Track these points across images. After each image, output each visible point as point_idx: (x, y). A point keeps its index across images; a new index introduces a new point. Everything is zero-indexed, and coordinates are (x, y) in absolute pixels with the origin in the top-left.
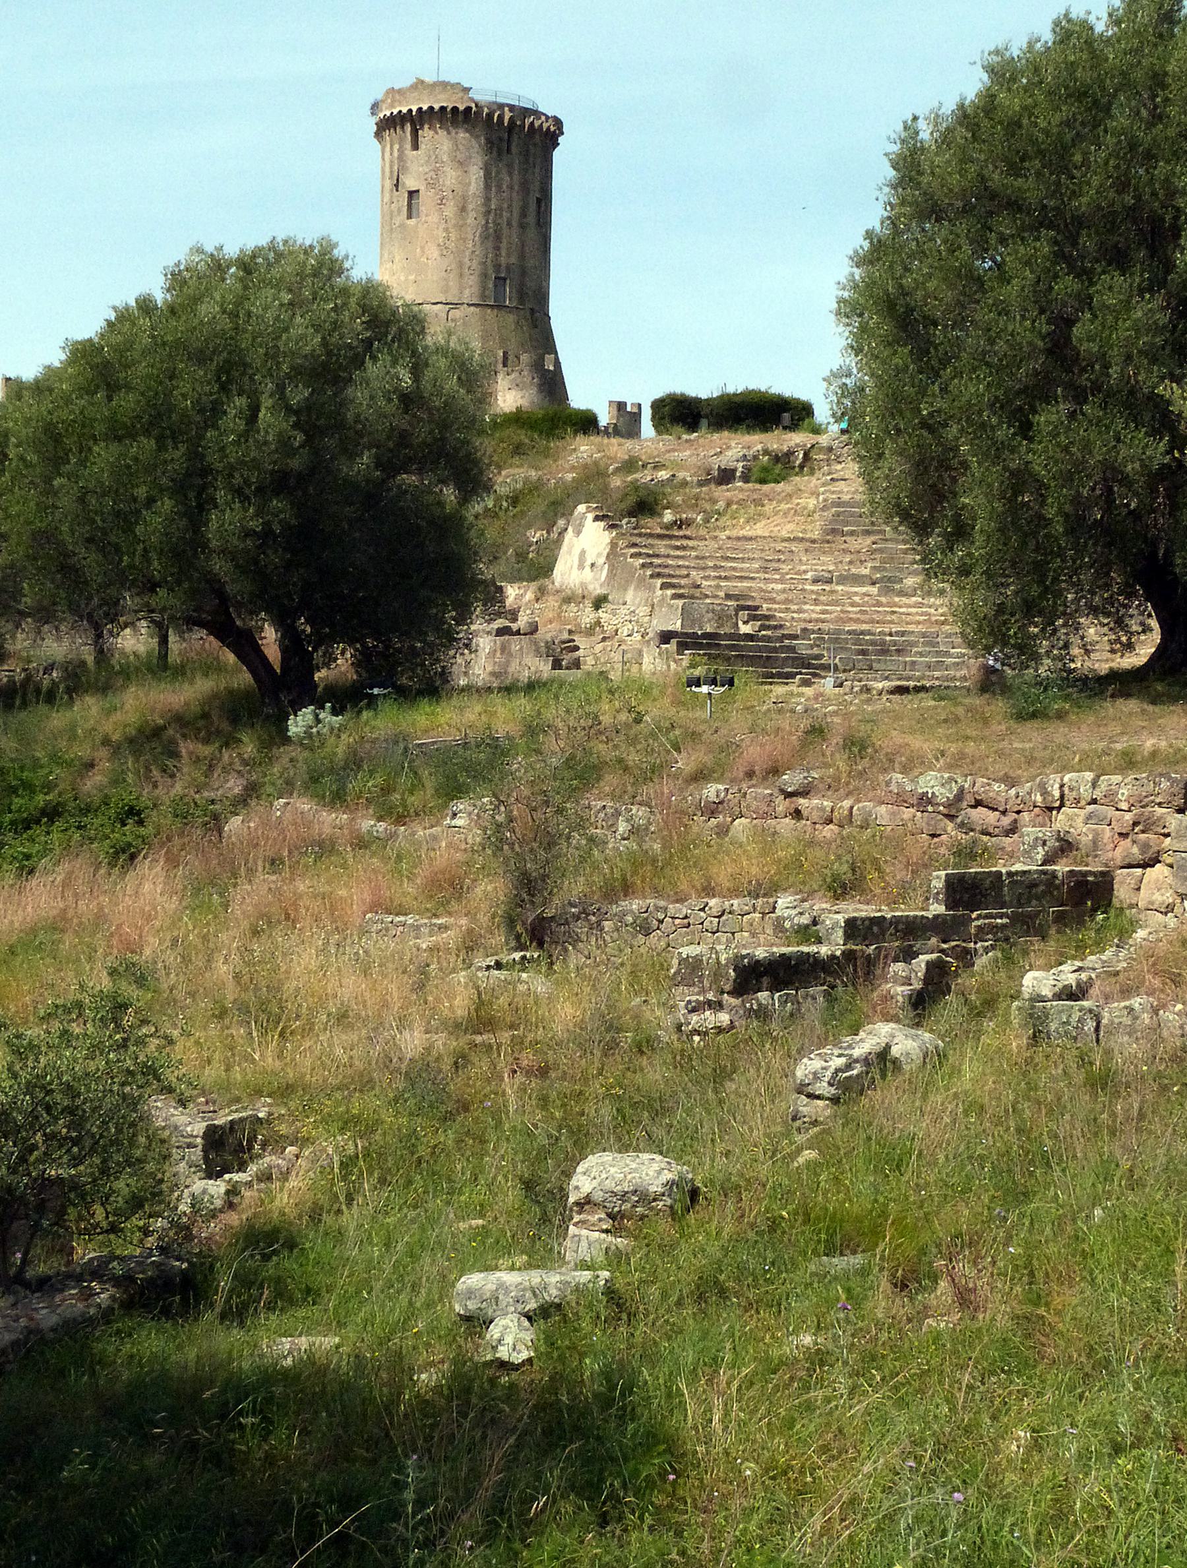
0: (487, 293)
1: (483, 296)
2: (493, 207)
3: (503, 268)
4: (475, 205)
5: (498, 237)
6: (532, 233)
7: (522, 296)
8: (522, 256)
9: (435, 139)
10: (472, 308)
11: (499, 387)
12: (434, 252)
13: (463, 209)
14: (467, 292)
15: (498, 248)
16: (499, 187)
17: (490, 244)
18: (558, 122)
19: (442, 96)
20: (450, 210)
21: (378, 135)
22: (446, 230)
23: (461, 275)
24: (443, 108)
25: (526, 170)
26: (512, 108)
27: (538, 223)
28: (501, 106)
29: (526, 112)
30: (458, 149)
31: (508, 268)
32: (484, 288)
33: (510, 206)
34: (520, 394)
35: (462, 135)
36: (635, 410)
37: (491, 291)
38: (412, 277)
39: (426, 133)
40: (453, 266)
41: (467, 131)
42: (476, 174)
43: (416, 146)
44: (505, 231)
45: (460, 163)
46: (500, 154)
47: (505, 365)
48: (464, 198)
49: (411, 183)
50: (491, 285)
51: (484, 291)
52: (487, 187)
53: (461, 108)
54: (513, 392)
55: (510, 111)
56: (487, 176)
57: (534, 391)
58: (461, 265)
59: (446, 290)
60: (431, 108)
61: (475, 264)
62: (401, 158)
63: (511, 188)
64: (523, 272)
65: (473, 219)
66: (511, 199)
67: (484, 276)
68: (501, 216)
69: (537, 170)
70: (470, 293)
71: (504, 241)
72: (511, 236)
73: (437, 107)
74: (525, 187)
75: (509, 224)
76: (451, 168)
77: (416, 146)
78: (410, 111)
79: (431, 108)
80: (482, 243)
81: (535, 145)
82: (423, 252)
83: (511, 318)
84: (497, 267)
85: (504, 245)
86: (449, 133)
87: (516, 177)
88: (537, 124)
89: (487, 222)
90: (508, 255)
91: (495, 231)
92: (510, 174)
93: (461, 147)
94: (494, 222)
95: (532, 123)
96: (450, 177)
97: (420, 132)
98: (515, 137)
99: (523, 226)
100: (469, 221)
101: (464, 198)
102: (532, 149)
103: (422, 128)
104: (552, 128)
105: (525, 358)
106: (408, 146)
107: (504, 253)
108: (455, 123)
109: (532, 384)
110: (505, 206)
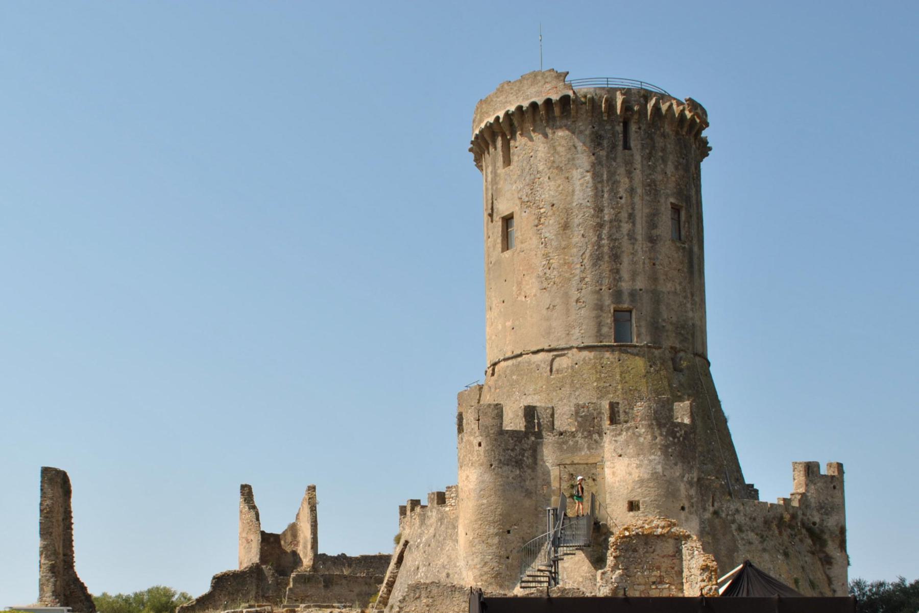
0: (605, 330)
1: (599, 335)
2: (607, 218)
3: (626, 297)
4: (581, 219)
5: (616, 257)
7: (656, 329)
8: (654, 279)
9: (532, 148)
10: (585, 353)
12: (532, 286)
13: (566, 226)
14: (576, 332)
15: (618, 271)
16: (614, 192)
17: (605, 266)
18: (694, 105)
19: (533, 90)
20: (550, 230)
21: (478, 160)
22: (546, 256)
23: (568, 310)
24: (534, 105)
25: (653, 168)
26: (627, 92)
27: (678, 237)
28: (612, 91)
29: (646, 95)
31: (633, 294)
32: (600, 325)
33: (631, 217)
34: (635, 462)
36: (833, 472)
37: (608, 329)
38: (509, 324)
39: (520, 143)
40: (558, 300)
42: (581, 181)
43: (507, 161)
45: (559, 169)
47: (613, 420)
48: (568, 212)
50: (609, 320)
51: (599, 331)
52: (598, 194)
53: (555, 97)
54: (625, 460)
55: (622, 94)
56: (596, 176)
57: (657, 457)
58: (566, 295)
59: (548, 332)
60: (520, 108)
61: (587, 294)
63: (632, 191)
64: (656, 298)
65: (581, 239)
67: (599, 307)
68: (619, 228)
69: (670, 169)
70: (582, 334)
71: (626, 260)
72: (636, 255)
73: (526, 104)
74: (652, 188)
76: (553, 175)
78: (498, 118)
79: (520, 108)
80: (594, 265)
81: (664, 135)
82: (520, 289)
83: (639, 364)
84: (617, 295)
86: (546, 136)
87: (638, 175)
88: (664, 107)
89: (600, 238)
91: (612, 249)
92: (629, 173)
93: (560, 149)
94: (610, 237)
95: (657, 108)
96: (549, 191)
97: (512, 143)
98: (633, 128)
99: (652, 240)
101: (568, 212)
102: (659, 142)
104: (688, 115)
105: (640, 408)
107: (625, 275)
109: (652, 446)
110: (624, 215)
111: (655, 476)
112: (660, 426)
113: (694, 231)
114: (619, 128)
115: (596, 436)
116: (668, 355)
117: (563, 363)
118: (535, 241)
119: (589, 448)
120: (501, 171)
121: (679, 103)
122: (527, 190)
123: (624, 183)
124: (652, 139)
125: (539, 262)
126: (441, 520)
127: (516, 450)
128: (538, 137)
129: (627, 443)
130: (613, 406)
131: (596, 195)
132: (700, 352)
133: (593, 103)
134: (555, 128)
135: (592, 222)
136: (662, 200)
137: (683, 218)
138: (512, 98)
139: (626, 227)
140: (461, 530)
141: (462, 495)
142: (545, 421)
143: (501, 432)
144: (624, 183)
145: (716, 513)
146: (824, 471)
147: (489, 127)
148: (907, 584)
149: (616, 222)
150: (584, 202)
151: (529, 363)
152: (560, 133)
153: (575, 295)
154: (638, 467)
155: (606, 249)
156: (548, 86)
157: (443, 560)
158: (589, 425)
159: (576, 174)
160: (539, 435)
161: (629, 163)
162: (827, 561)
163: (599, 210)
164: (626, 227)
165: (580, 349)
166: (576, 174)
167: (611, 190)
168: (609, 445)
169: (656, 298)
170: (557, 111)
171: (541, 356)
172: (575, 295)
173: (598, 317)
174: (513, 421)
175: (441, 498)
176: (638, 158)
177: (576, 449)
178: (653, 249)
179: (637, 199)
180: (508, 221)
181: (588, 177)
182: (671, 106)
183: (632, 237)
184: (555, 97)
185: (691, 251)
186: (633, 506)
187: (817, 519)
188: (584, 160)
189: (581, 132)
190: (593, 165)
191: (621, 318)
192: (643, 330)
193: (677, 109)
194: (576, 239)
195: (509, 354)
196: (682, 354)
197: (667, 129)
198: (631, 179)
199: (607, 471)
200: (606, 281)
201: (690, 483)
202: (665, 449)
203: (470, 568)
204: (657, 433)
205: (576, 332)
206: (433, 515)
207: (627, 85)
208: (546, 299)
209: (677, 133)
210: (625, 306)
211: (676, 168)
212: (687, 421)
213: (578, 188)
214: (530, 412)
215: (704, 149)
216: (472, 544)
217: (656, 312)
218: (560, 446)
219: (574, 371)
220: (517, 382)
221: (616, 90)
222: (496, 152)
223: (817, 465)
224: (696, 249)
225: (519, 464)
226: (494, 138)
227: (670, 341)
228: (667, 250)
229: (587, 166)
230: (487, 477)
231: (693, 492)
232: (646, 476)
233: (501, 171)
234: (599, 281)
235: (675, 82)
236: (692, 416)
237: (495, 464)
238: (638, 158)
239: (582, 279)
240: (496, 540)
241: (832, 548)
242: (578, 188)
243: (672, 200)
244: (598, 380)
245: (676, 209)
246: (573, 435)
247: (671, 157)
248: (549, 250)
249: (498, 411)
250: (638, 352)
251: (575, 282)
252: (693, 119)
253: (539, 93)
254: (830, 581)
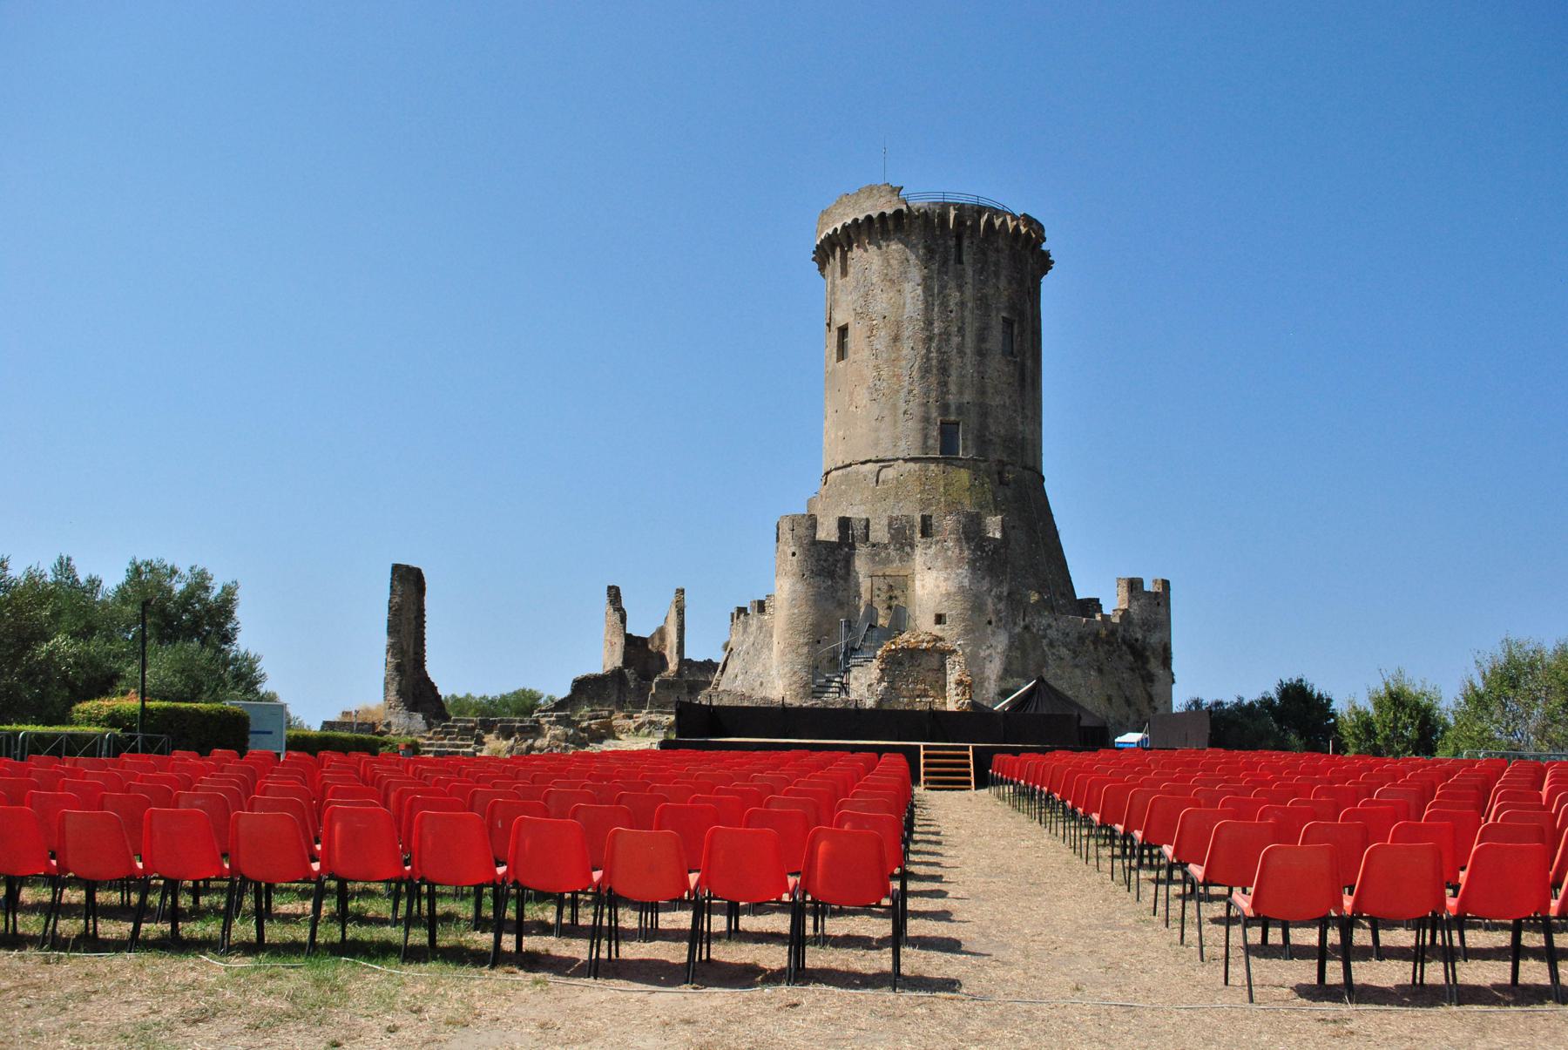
0: (931, 442)
1: (925, 447)
3: (953, 408)
5: (944, 370)
7: (982, 443)
9: (867, 259)
10: (911, 465)
11: (918, 568)
12: (862, 397)
13: (896, 339)
14: (903, 444)
15: (946, 384)
16: (944, 305)
17: (933, 380)
20: (882, 340)
22: (877, 367)
24: (869, 218)
25: (985, 283)
26: (960, 208)
27: (1009, 352)
28: (945, 206)
29: (980, 210)
30: (889, 264)
31: (960, 408)
32: (926, 437)
33: (961, 330)
34: (943, 575)
36: (1158, 589)
37: (934, 441)
38: (841, 434)
39: (856, 253)
40: (886, 412)
41: (900, 241)
42: (912, 294)
43: (844, 273)
44: (956, 361)
46: (944, 263)
48: (898, 324)
49: (840, 319)
50: (935, 432)
52: (928, 307)
53: (889, 211)
54: (934, 573)
56: (927, 289)
57: (964, 571)
60: (856, 220)
61: (915, 407)
63: (962, 304)
64: (984, 412)
66: (963, 318)
67: (926, 420)
68: (948, 340)
69: (1003, 284)
70: (909, 444)
72: (963, 368)
73: (861, 217)
74: (983, 303)
75: (961, 351)
76: (887, 286)
77: (844, 273)
79: (856, 220)
80: (922, 377)
81: (997, 250)
83: (964, 476)
84: (944, 408)
85: (953, 378)
86: (880, 248)
87: (969, 290)
88: (998, 222)
90: (961, 393)
91: (940, 362)
92: (960, 288)
94: (939, 350)
95: (990, 223)
96: (882, 302)
98: (966, 243)
99: (981, 353)
100: (904, 352)
101: (899, 324)
102: (992, 257)
103: (850, 249)
104: (1023, 230)
106: (838, 274)
107: (953, 388)
109: (961, 559)
111: (961, 589)
112: (968, 539)
113: (1028, 345)
114: (952, 243)
115: (908, 549)
116: (994, 468)
117: (889, 474)
118: (867, 352)
119: (901, 560)
120: (839, 282)
121: (1014, 217)
122: (861, 301)
123: (954, 297)
124: (985, 254)
125: (870, 373)
126: (760, 628)
127: (829, 561)
128: (872, 249)
129: (936, 556)
130: (926, 520)
131: (926, 309)
132: (1031, 464)
133: (926, 216)
134: (888, 239)
135: (920, 336)
136: (993, 314)
137: (1016, 331)
138: (848, 210)
139: (956, 340)
140: (775, 639)
141: (777, 604)
142: (858, 530)
143: (815, 543)
144: (954, 297)
145: (1026, 628)
146: (1148, 586)
147: (829, 237)
148: (1246, 702)
149: (945, 336)
150: (915, 315)
151: (857, 473)
152: (895, 246)
153: (903, 407)
154: (946, 580)
155: (934, 362)
156: (883, 200)
157: (758, 669)
158: (902, 538)
159: (908, 287)
160: (852, 547)
161: (960, 277)
162: (1149, 678)
163: (929, 323)
164: (956, 340)
165: (906, 460)
166: (908, 287)
167: (941, 304)
168: (919, 557)
169: (984, 412)
170: (891, 225)
171: (869, 465)
172: (903, 407)
173: (924, 429)
174: (827, 532)
175: (761, 607)
176: (969, 272)
177: (888, 561)
178: (981, 363)
179: (967, 313)
180: (843, 331)
181: (919, 290)
182: (1004, 222)
183: (961, 351)
184: (889, 211)
185: (1023, 365)
186: (939, 619)
187: (1139, 636)
188: (916, 274)
189: (914, 246)
190: (925, 279)
191: (948, 433)
192: (970, 443)
193: (1011, 225)
194: (906, 350)
195: (840, 464)
196: (1009, 467)
197: (1001, 243)
198: (962, 293)
199: (918, 584)
200: (933, 394)
201: (999, 598)
202: (972, 564)
203: (781, 677)
204: (965, 547)
205: (903, 444)
206: (754, 622)
207: (962, 200)
208: (876, 411)
209: (1012, 248)
210: (953, 418)
211: (1010, 283)
212: (998, 535)
213: (909, 301)
214: (844, 524)
215: (1045, 263)
216: (783, 654)
217: (983, 427)
218: (872, 557)
219: (899, 483)
220: (845, 492)
221: (949, 204)
222: (835, 263)
223: (1141, 581)
224: (1029, 363)
225: (831, 575)
226: (832, 249)
227: (997, 454)
228: (997, 366)
229: (918, 279)
230: (799, 587)
231: (1001, 606)
232: (953, 590)
233: (839, 282)
234: (927, 394)
235: (1011, 195)
236: (1004, 531)
237: (807, 574)
238: (969, 272)
239: (910, 392)
240: (805, 650)
241: (1154, 666)
242: (909, 301)
243: (1004, 314)
244: (921, 492)
245: (1008, 323)
246: (886, 547)
247: (1004, 272)
248: (880, 361)
249: (812, 522)
250: (964, 464)
251: (903, 393)
252: (1028, 233)
253: (874, 207)
254: (1151, 698)
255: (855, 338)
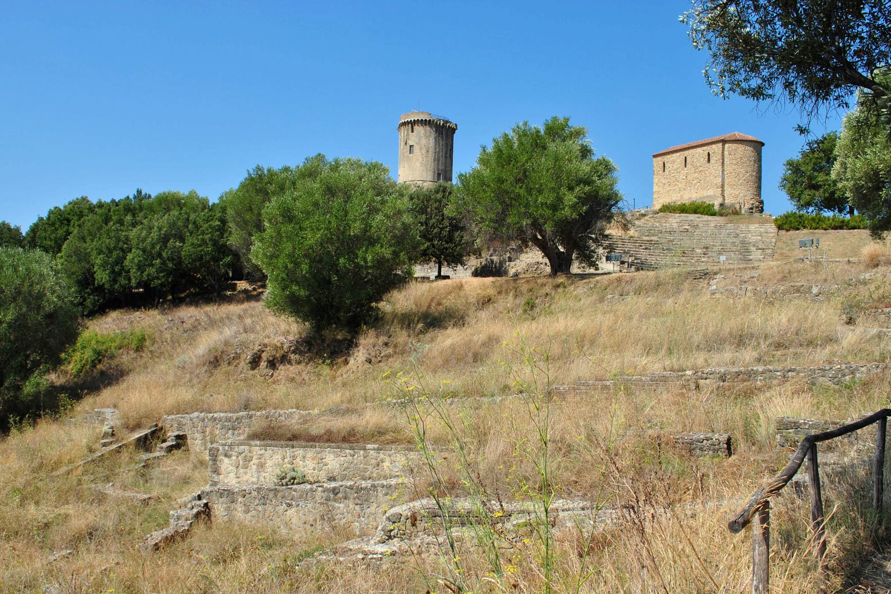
4: (431, 150)
6: (448, 159)
12: (418, 164)
20: (424, 151)
29: (447, 122)
35: (428, 128)
39: (416, 127)
42: (432, 141)
43: (413, 131)
49: (410, 143)
62: (408, 135)
65: (431, 155)
70: (430, 178)
72: (442, 160)
74: (447, 144)
76: (423, 139)
77: (413, 131)
96: (424, 141)
99: (446, 157)
108: (426, 124)
188: (433, 136)
191: (439, 175)
255: (416, 149)
